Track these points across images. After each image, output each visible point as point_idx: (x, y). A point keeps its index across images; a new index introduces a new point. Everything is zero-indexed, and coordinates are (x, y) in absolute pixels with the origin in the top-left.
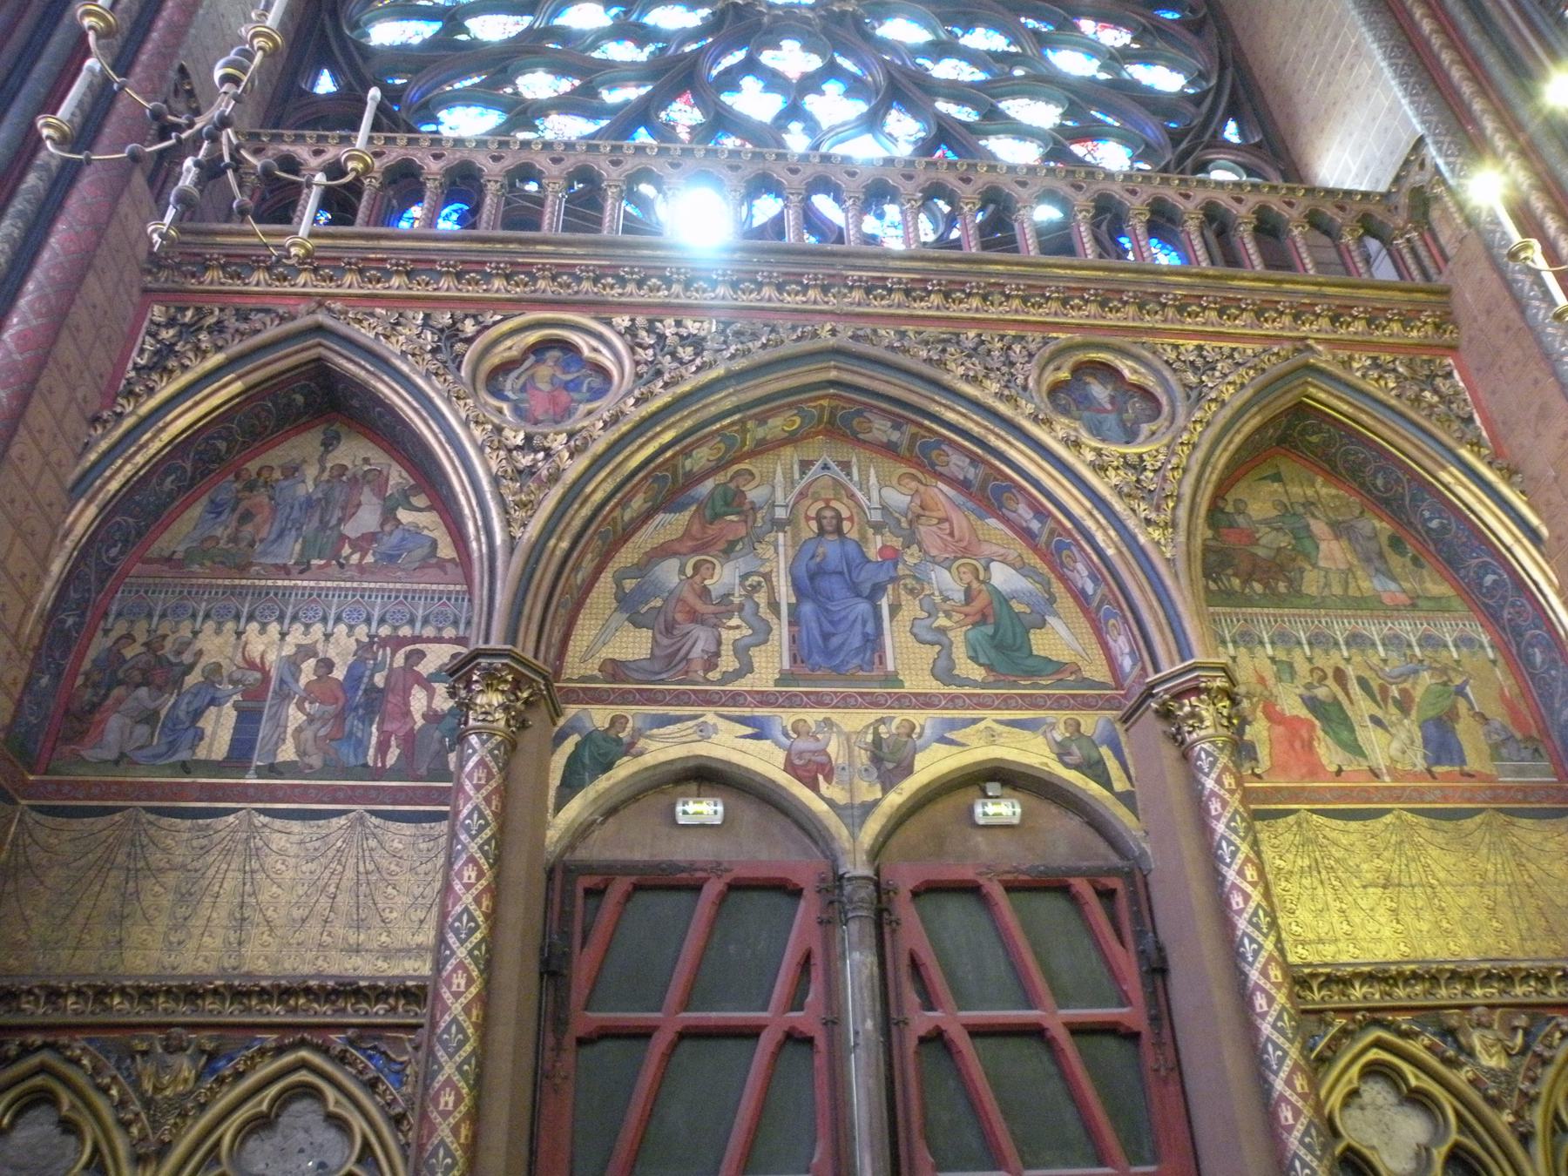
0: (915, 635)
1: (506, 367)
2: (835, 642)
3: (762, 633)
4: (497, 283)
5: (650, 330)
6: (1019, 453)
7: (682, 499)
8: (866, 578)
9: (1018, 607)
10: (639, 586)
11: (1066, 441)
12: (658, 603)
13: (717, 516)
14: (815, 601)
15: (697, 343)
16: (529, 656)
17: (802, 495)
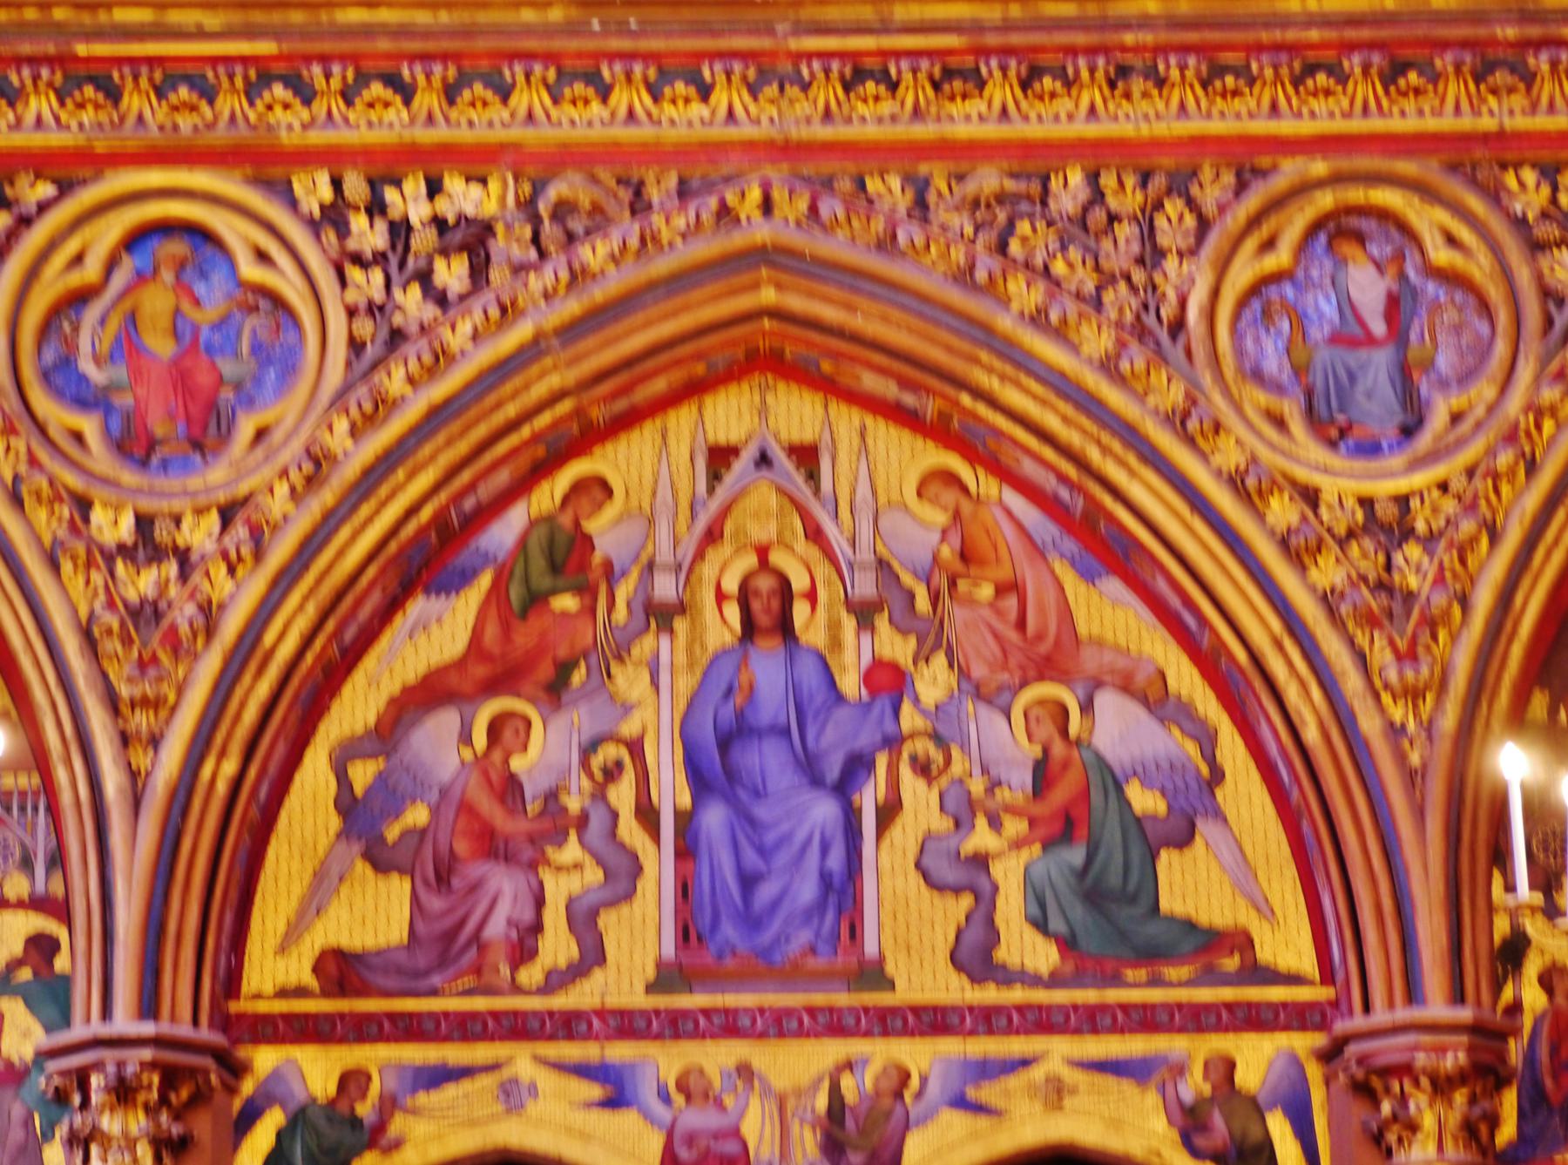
0: (926, 876)
1: (79, 298)
2: (765, 892)
3: (623, 875)
4: (39, 104)
5: (376, 208)
6: (1146, 490)
7: (463, 558)
8: (833, 741)
9: (1145, 800)
10: (381, 778)
11: (1235, 483)
12: (417, 815)
13: (536, 601)
14: (732, 801)
15: (472, 240)
16: (184, 1030)
17: (713, 535)
